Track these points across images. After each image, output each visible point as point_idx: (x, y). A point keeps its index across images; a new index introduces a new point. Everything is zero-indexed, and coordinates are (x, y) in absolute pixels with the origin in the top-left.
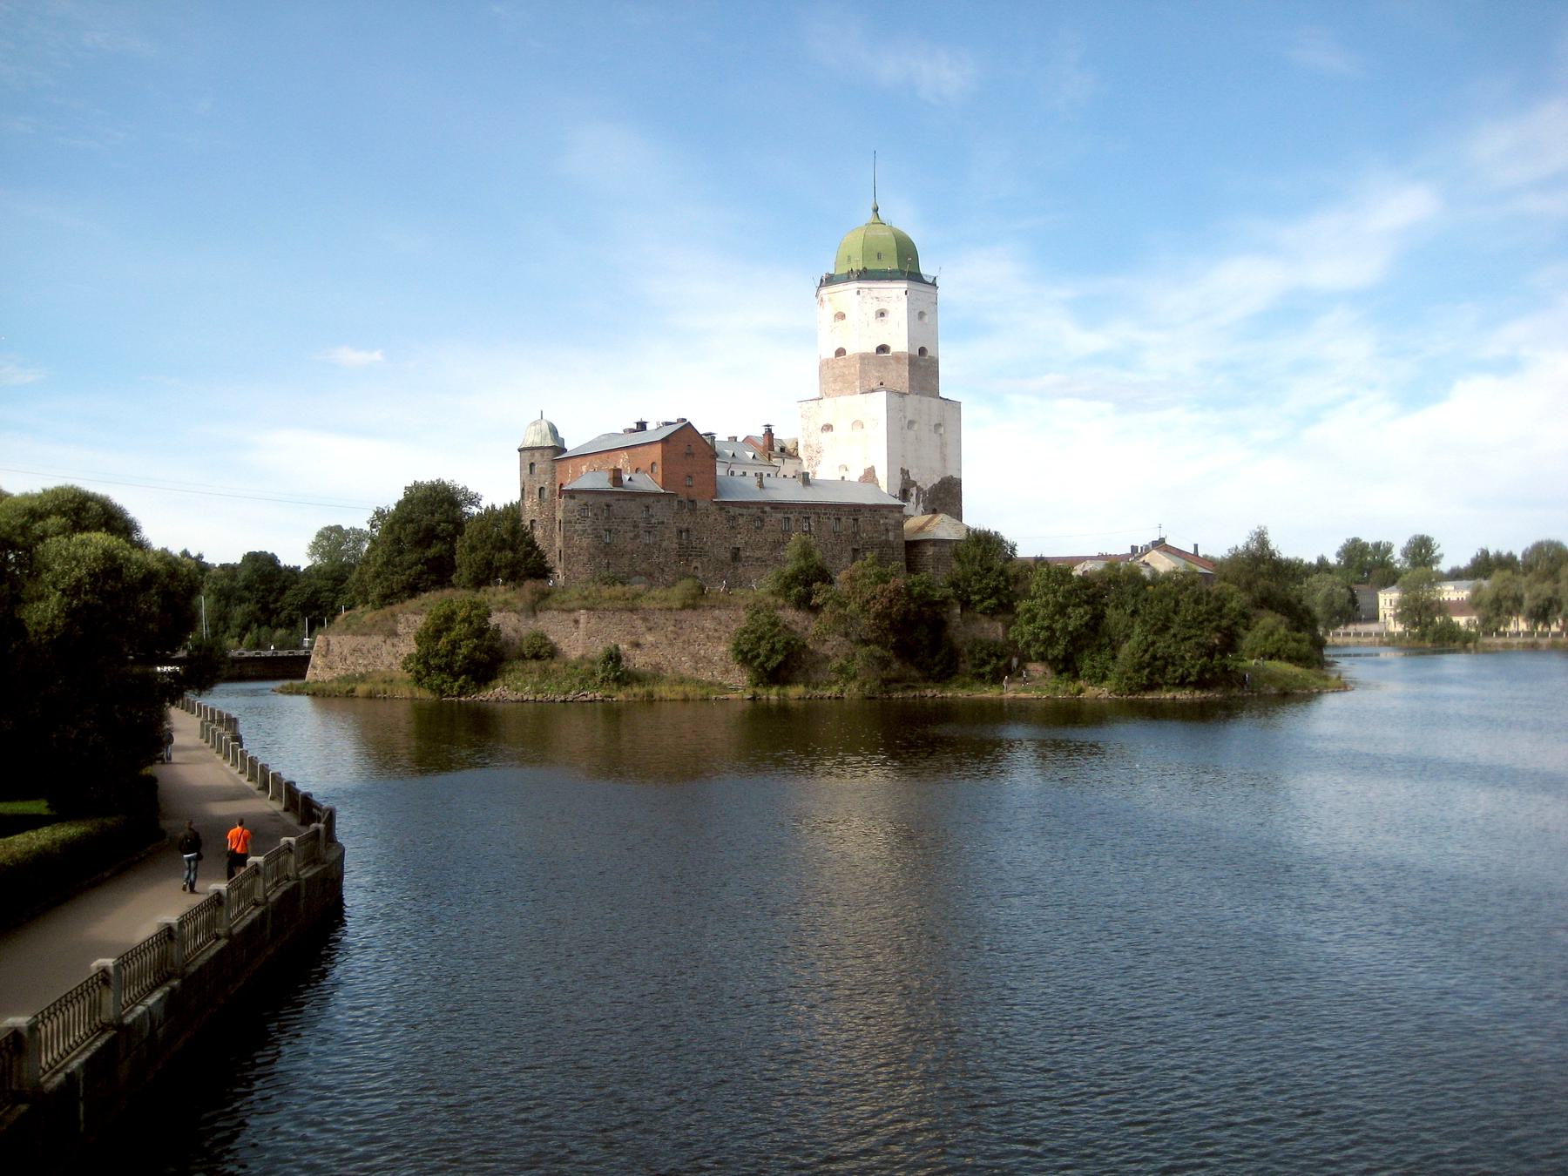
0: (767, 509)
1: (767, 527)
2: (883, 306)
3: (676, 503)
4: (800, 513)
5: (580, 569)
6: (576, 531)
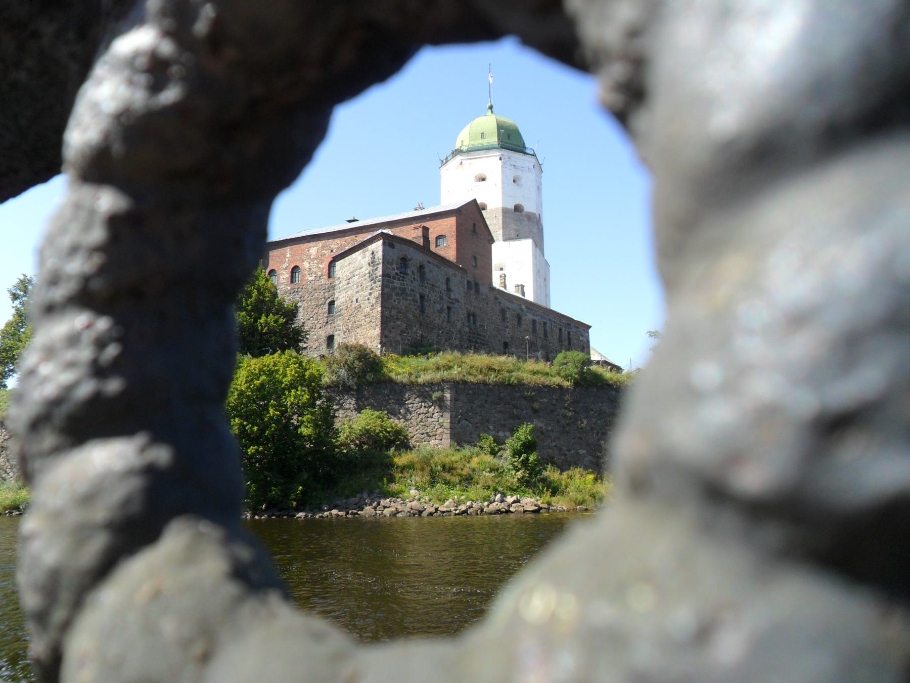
0: (523, 307)
1: (524, 327)
2: (519, 173)
3: (466, 281)
4: (542, 317)
5: (399, 338)
6: (395, 288)
